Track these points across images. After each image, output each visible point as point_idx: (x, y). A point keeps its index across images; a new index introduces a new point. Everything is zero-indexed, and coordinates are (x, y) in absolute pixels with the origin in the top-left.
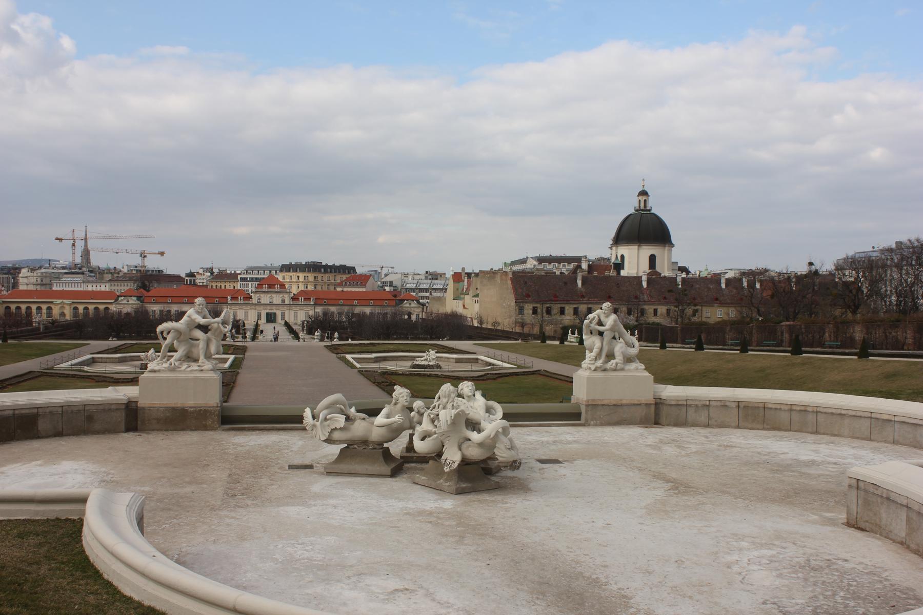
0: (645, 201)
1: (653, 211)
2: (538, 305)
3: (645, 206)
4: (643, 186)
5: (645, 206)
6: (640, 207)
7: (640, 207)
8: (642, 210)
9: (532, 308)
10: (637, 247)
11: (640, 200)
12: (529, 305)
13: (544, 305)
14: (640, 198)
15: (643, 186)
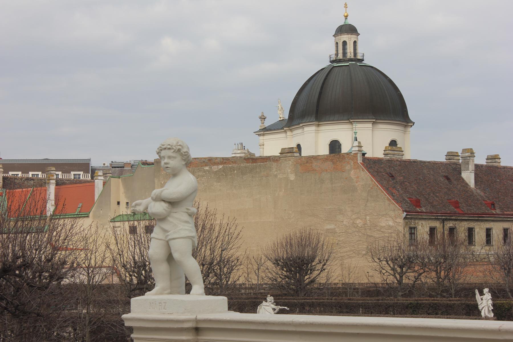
0: (355, 42)
1: (367, 62)
2: (436, 224)
3: (355, 54)
4: (346, 17)
5: (355, 54)
6: (344, 53)
7: (344, 53)
8: (351, 60)
9: (427, 229)
10: (370, 125)
11: (345, 43)
12: (424, 222)
13: (446, 223)
14: (345, 37)
15: (346, 17)
